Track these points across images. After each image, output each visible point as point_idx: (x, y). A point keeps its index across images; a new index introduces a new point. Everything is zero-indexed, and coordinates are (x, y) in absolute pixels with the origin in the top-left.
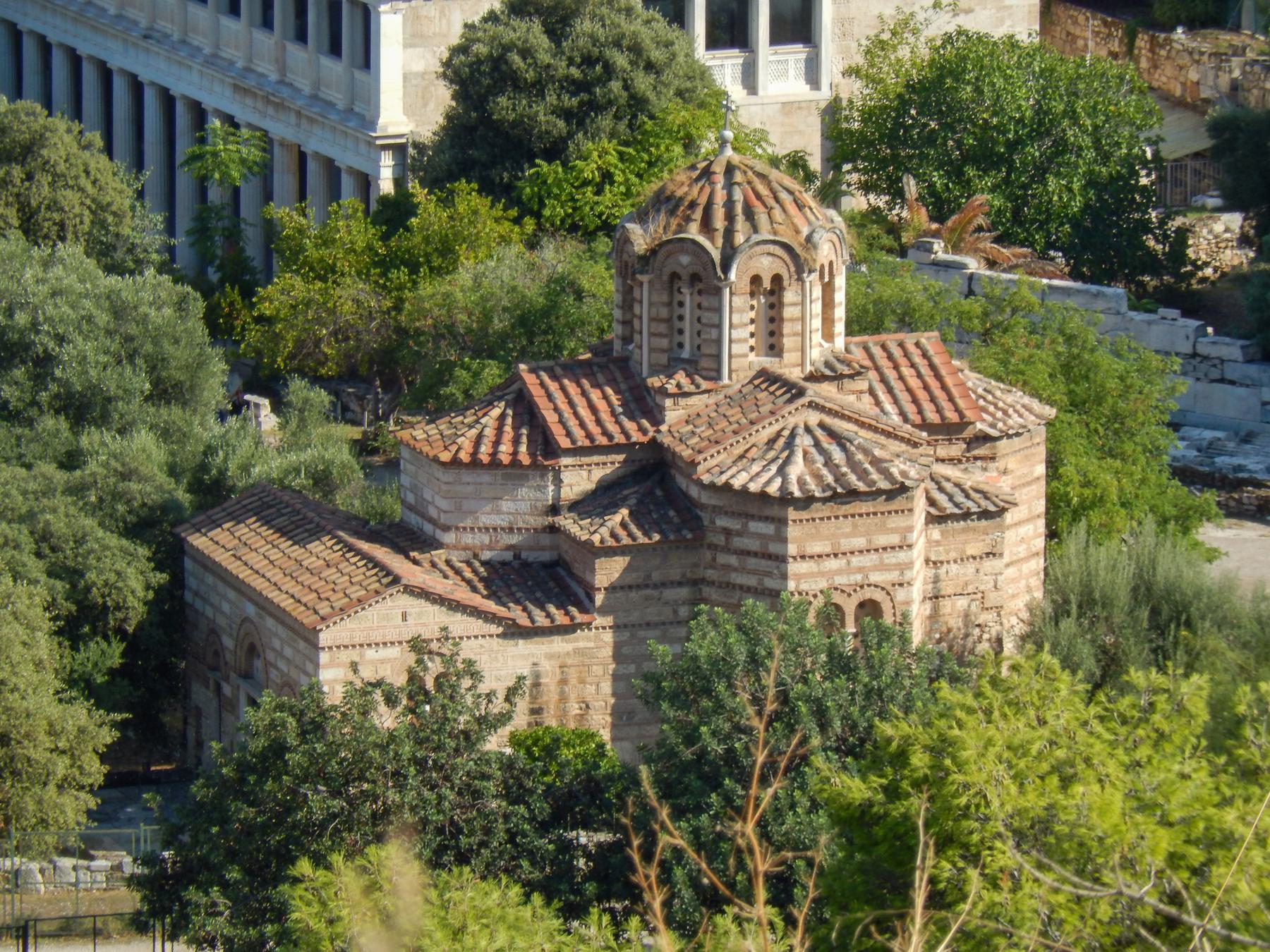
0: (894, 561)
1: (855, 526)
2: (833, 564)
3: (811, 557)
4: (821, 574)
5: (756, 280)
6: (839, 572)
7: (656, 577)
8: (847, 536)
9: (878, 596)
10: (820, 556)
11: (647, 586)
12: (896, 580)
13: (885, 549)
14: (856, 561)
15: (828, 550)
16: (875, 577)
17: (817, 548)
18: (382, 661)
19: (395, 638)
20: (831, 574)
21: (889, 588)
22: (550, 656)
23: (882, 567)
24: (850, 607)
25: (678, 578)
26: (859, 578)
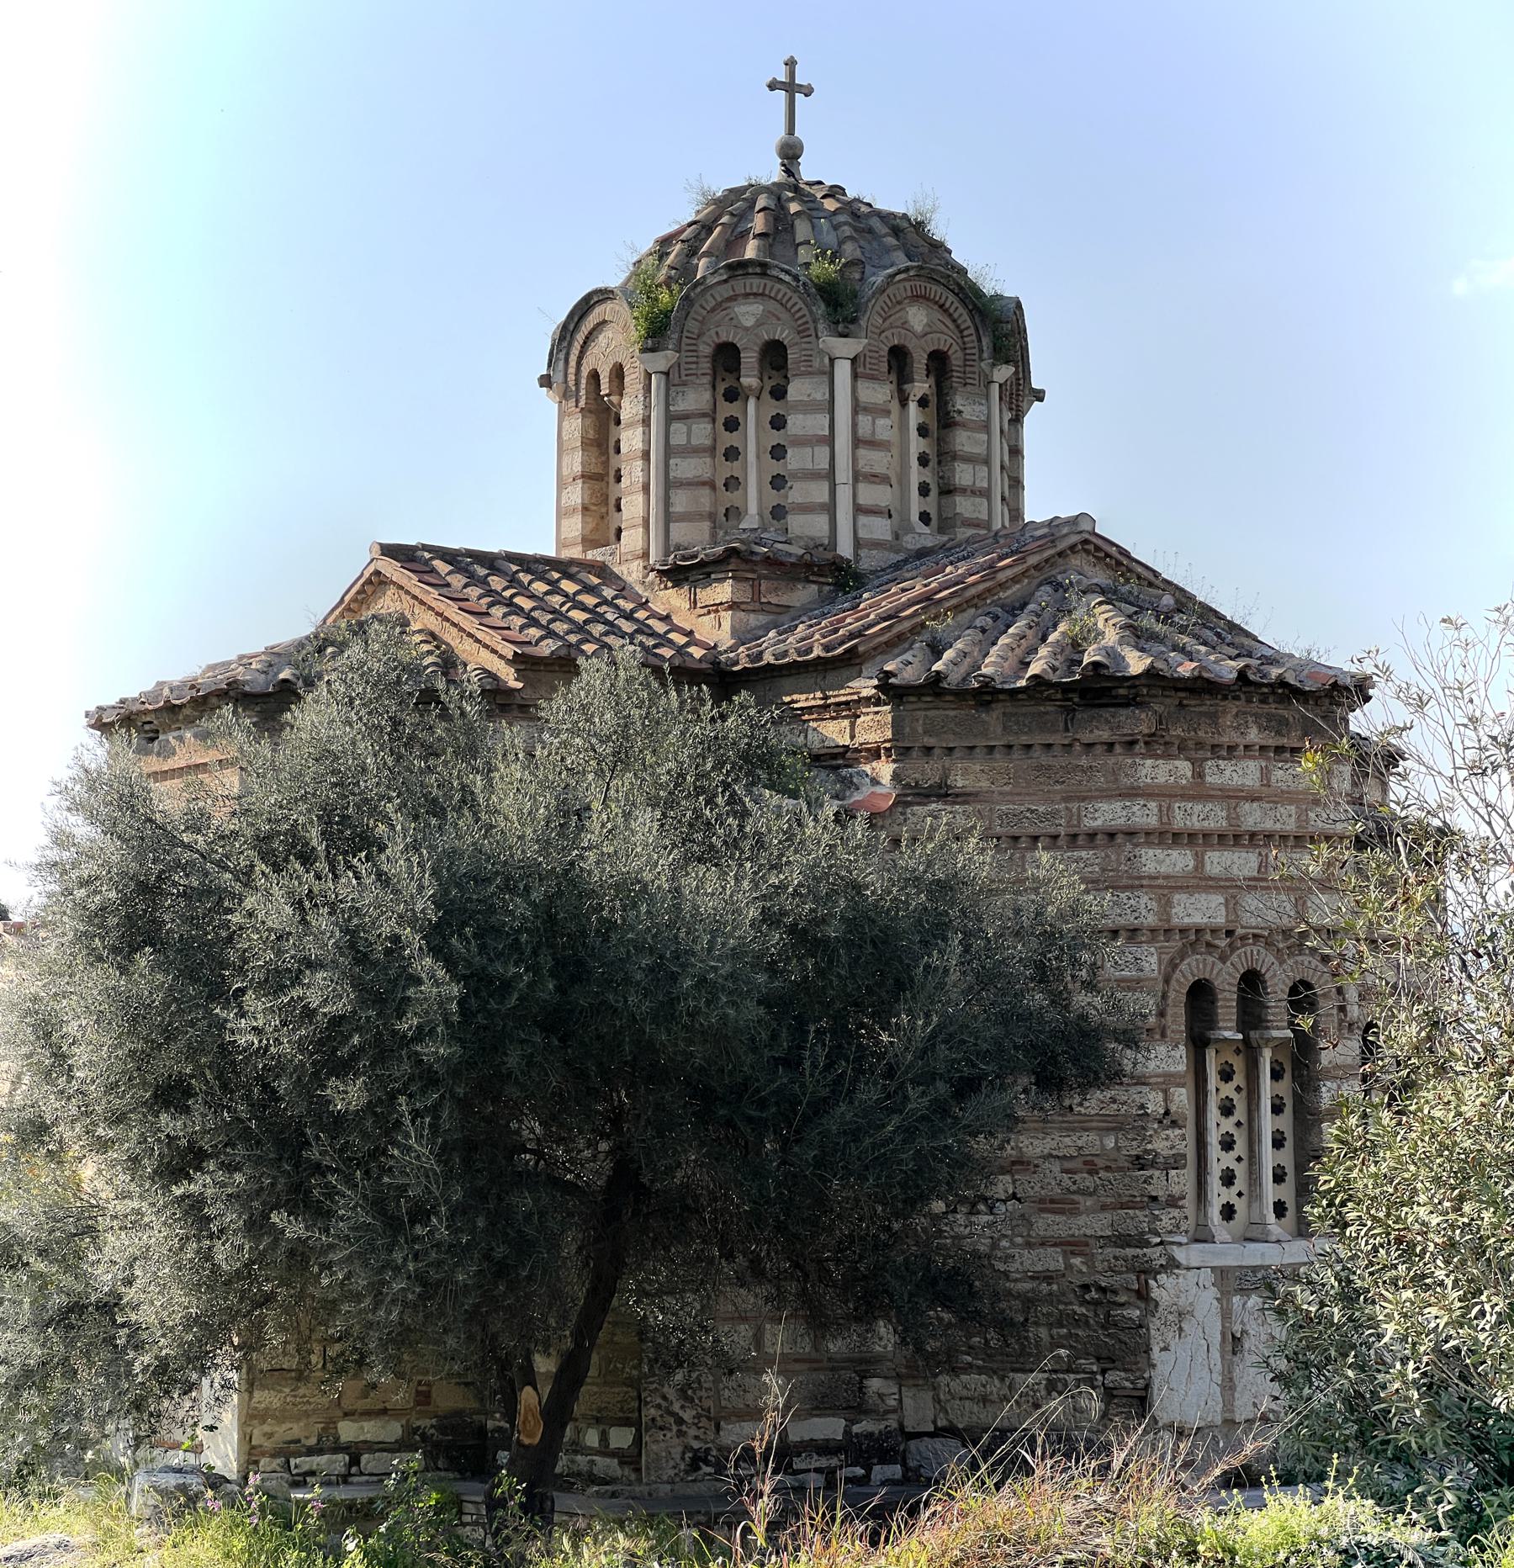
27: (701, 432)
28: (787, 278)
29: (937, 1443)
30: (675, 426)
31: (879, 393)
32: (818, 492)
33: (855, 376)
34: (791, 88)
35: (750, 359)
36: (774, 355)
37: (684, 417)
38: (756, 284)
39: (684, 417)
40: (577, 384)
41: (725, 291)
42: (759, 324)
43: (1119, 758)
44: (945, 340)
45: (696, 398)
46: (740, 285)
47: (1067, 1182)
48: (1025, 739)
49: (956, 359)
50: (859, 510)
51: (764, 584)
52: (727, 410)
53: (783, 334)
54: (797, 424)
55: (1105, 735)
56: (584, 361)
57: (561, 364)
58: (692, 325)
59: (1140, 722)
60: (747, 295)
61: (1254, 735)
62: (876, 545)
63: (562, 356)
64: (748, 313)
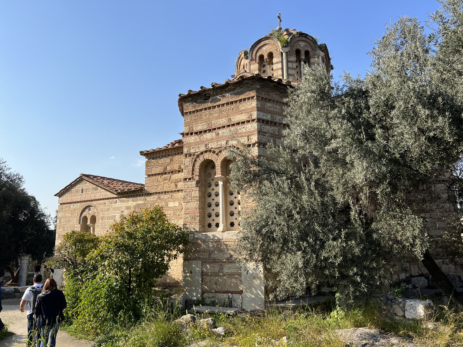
0: (244, 130)
1: (221, 112)
2: (208, 136)
3: (196, 133)
5: (262, 57)
7: (169, 168)
8: (217, 118)
10: (201, 132)
11: (166, 173)
12: (246, 143)
13: (238, 124)
14: (220, 132)
15: (205, 128)
17: (199, 128)
19: (79, 200)
22: (128, 208)
25: (177, 168)
27: (295, 65)
28: (311, 38)
29: (419, 278)
30: (289, 63)
35: (303, 53)
37: (291, 62)
38: (304, 39)
39: (291, 62)
40: (256, 57)
41: (298, 39)
42: (304, 46)
45: (293, 58)
46: (301, 38)
47: (442, 215)
53: (309, 49)
56: (258, 53)
57: (251, 54)
58: (292, 44)
60: (302, 40)
63: (251, 52)
64: (302, 44)
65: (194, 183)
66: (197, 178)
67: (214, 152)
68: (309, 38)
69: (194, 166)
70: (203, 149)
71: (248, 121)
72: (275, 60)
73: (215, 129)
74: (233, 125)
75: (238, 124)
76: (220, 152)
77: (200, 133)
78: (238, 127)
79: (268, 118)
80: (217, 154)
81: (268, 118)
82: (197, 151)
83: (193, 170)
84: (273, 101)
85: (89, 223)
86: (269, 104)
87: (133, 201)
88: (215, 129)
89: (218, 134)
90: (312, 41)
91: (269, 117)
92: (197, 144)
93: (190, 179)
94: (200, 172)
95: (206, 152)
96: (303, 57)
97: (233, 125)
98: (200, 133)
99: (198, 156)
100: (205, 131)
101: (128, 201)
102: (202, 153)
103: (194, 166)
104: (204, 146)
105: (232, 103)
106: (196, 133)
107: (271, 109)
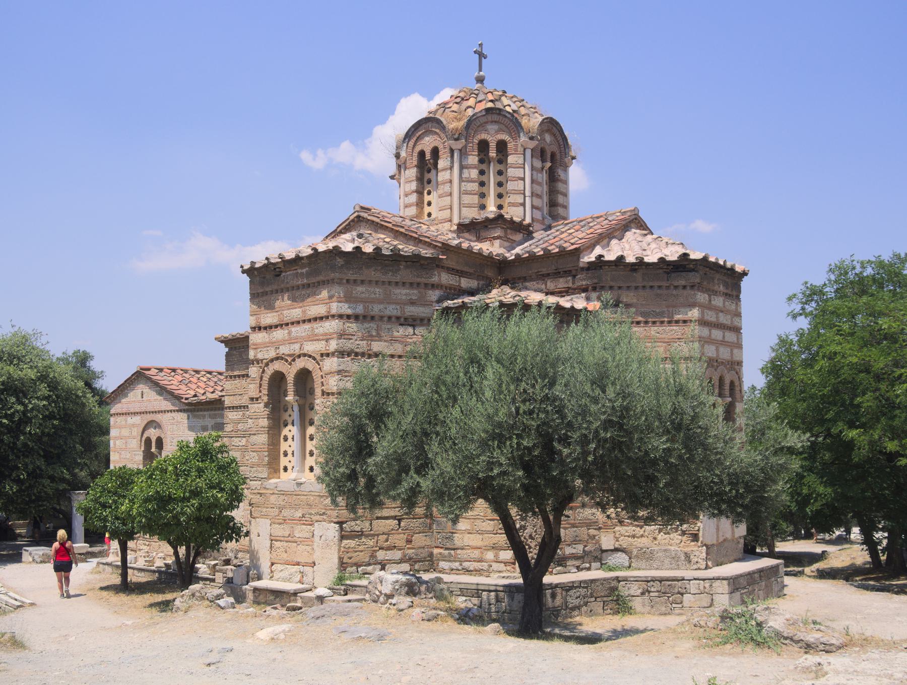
2: (279, 334)
3: (265, 328)
4: (271, 343)
5: (422, 154)
6: (283, 342)
9: (310, 365)
10: (271, 327)
13: (315, 319)
14: (294, 329)
16: (309, 347)
18: (133, 425)
20: (276, 345)
21: (318, 358)
23: (314, 338)
24: (290, 378)
26: (295, 348)
30: (465, 171)
31: (538, 164)
32: (520, 199)
33: (532, 156)
34: (481, 55)
36: (502, 147)
38: (496, 117)
43: (688, 291)
44: (555, 148)
46: (490, 118)
48: (651, 284)
49: (558, 156)
50: (533, 207)
51: (509, 231)
52: (484, 167)
54: (511, 172)
55: (683, 283)
59: (695, 278)
60: (492, 122)
61: (722, 288)
62: (538, 221)
65: (262, 405)
66: (265, 398)
67: (287, 361)
68: (506, 116)
69: (261, 378)
70: (272, 354)
71: (327, 317)
72: (442, 164)
73: (287, 324)
74: (309, 321)
75: (315, 319)
76: (294, 360)
77: (269, 328)
78: (315, 325)
79: (357, 310)
80: (290, 364)
81: (357, 310)
82: (266, 357)
83: (261, 385)
84: (370, 281)
85: (153, 449)
86: (360, 289)
87: (210, 416)
88: (287, 324)
89: (289, 333)
90: (511, 121)
91: (360, 309)
92: (266, 345)
93: (257, 399)
94: (269, 390)
95: (277, 359)
96: (493, 154)
97: (309, 321)
98: (269, 328)
99: (267, 365)
100: (276, 326)
101: (204, 416)
102: (272, 360)
103: (261, 378)
104: (273, 349)
105: (309, 285)
106: (265, 328)
107: (363, 295)
